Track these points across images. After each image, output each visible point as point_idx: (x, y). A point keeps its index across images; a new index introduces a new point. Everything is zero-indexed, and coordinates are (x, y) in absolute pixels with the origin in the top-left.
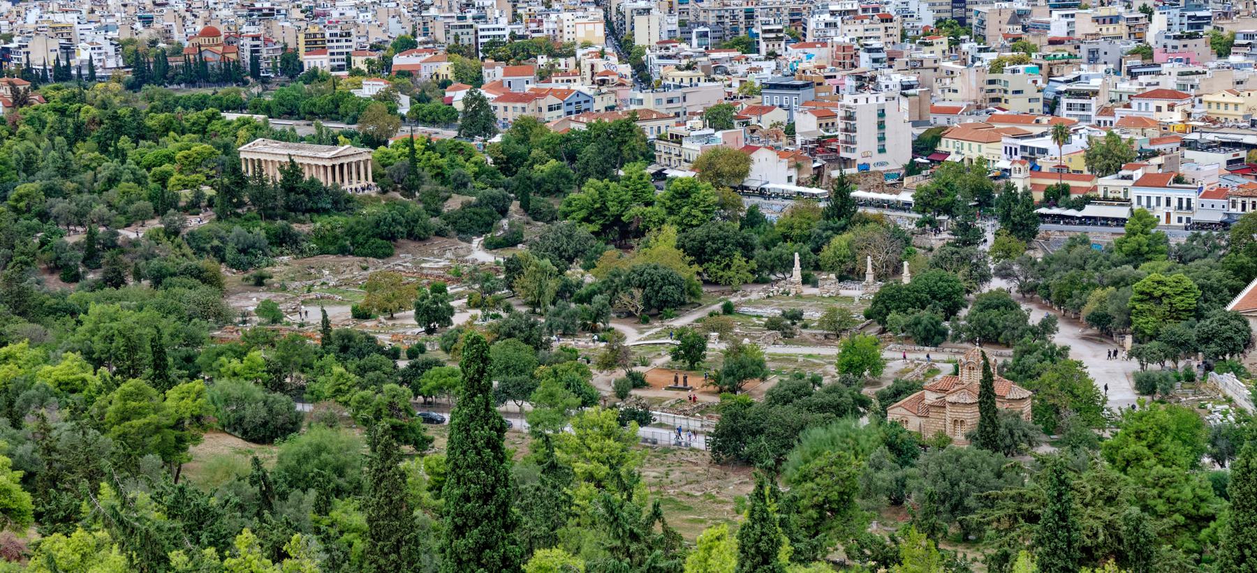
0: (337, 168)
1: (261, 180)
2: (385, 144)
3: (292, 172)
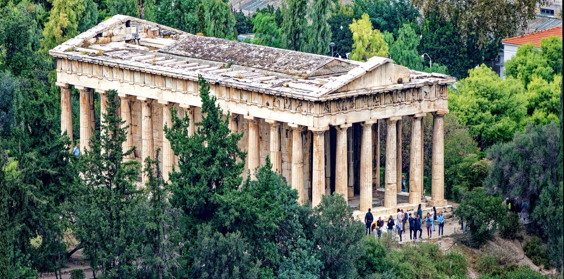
0: (342, 140)
1: (115, 172)
2: (492, 58)
3: (210, 145)
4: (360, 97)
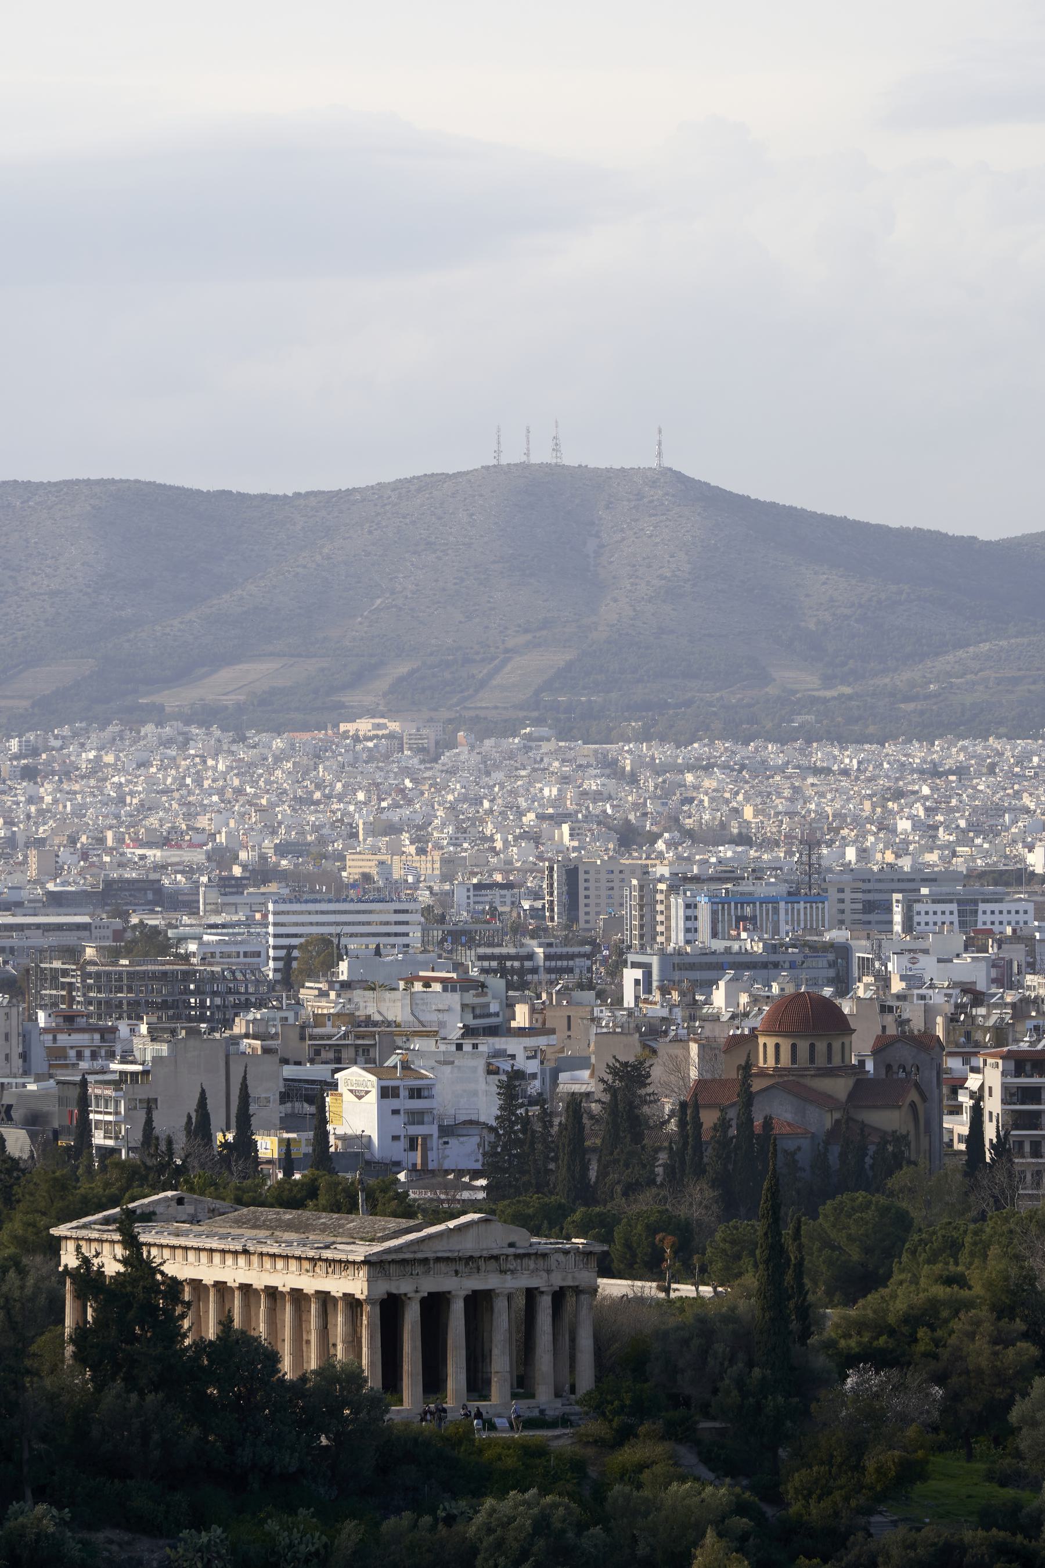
4: (438, 1260)
